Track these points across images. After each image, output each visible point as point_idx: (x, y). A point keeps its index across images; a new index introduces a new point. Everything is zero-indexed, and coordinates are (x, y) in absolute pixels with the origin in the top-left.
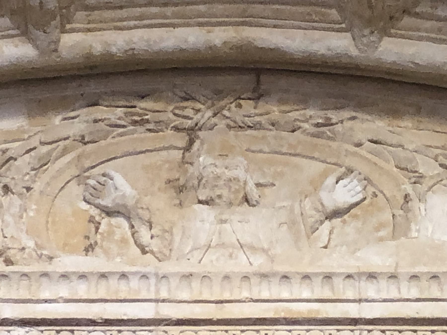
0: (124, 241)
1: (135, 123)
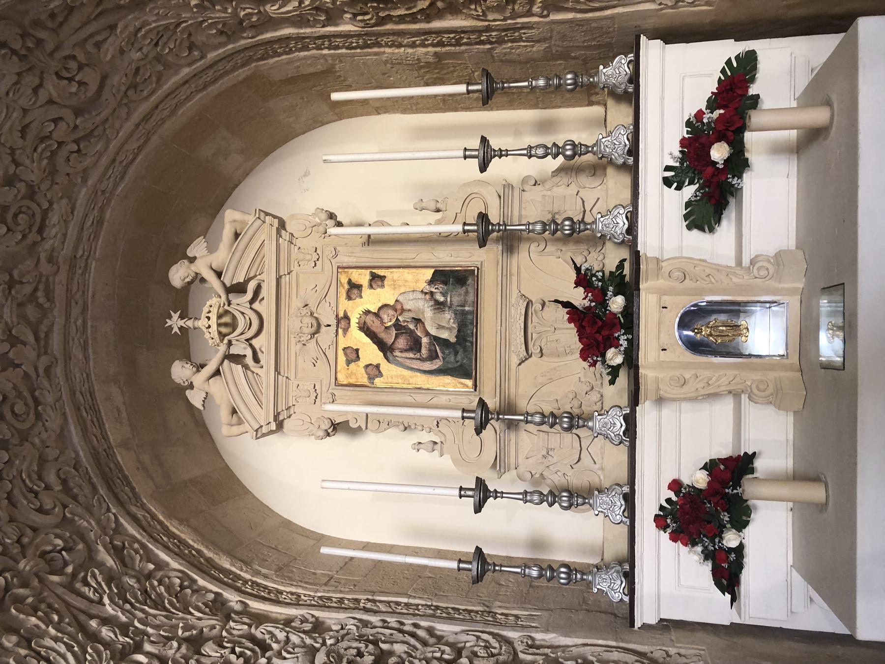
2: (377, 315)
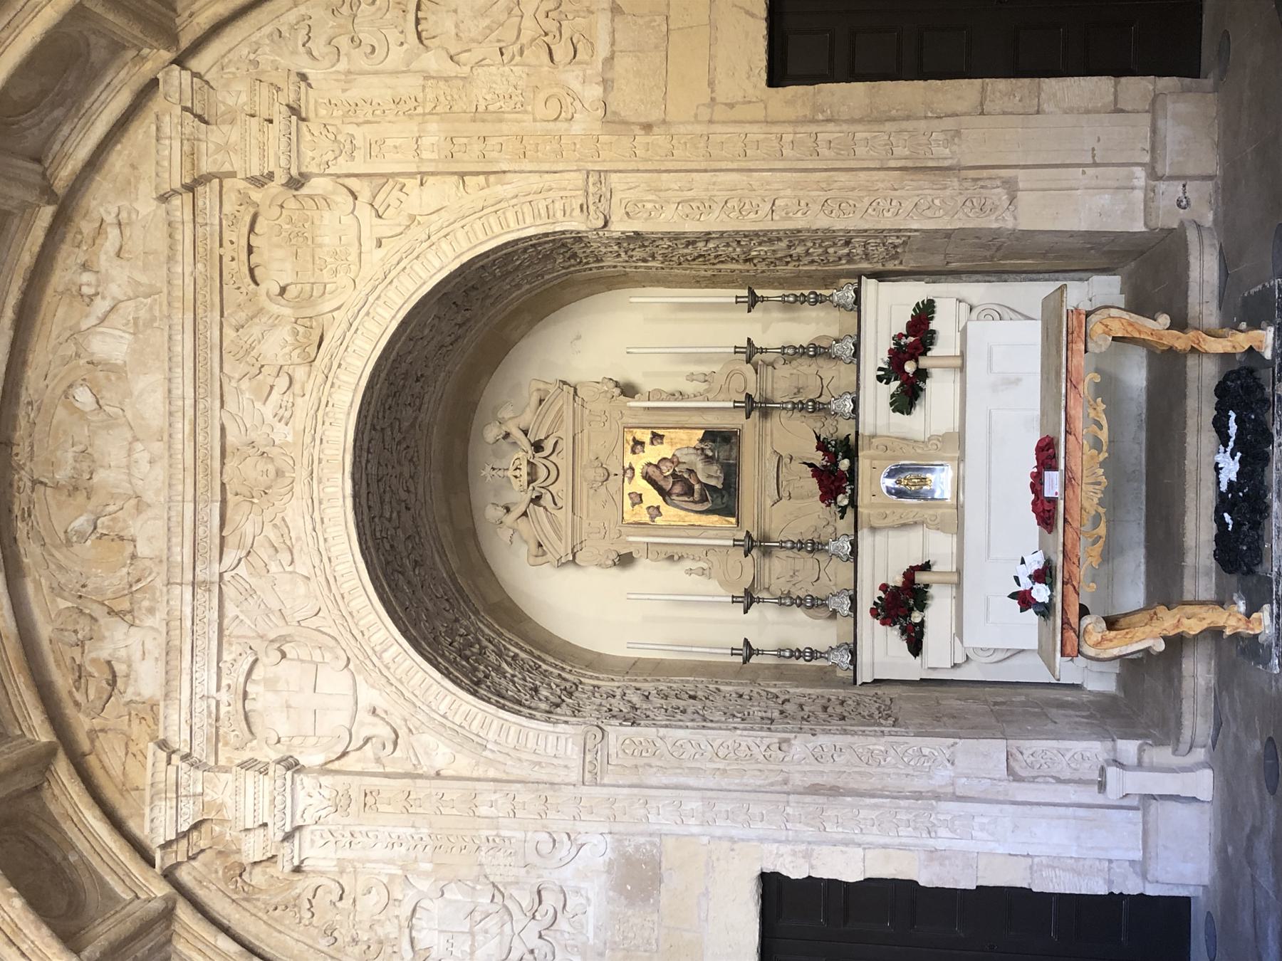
0: (112, 520)
1: (30, 515)
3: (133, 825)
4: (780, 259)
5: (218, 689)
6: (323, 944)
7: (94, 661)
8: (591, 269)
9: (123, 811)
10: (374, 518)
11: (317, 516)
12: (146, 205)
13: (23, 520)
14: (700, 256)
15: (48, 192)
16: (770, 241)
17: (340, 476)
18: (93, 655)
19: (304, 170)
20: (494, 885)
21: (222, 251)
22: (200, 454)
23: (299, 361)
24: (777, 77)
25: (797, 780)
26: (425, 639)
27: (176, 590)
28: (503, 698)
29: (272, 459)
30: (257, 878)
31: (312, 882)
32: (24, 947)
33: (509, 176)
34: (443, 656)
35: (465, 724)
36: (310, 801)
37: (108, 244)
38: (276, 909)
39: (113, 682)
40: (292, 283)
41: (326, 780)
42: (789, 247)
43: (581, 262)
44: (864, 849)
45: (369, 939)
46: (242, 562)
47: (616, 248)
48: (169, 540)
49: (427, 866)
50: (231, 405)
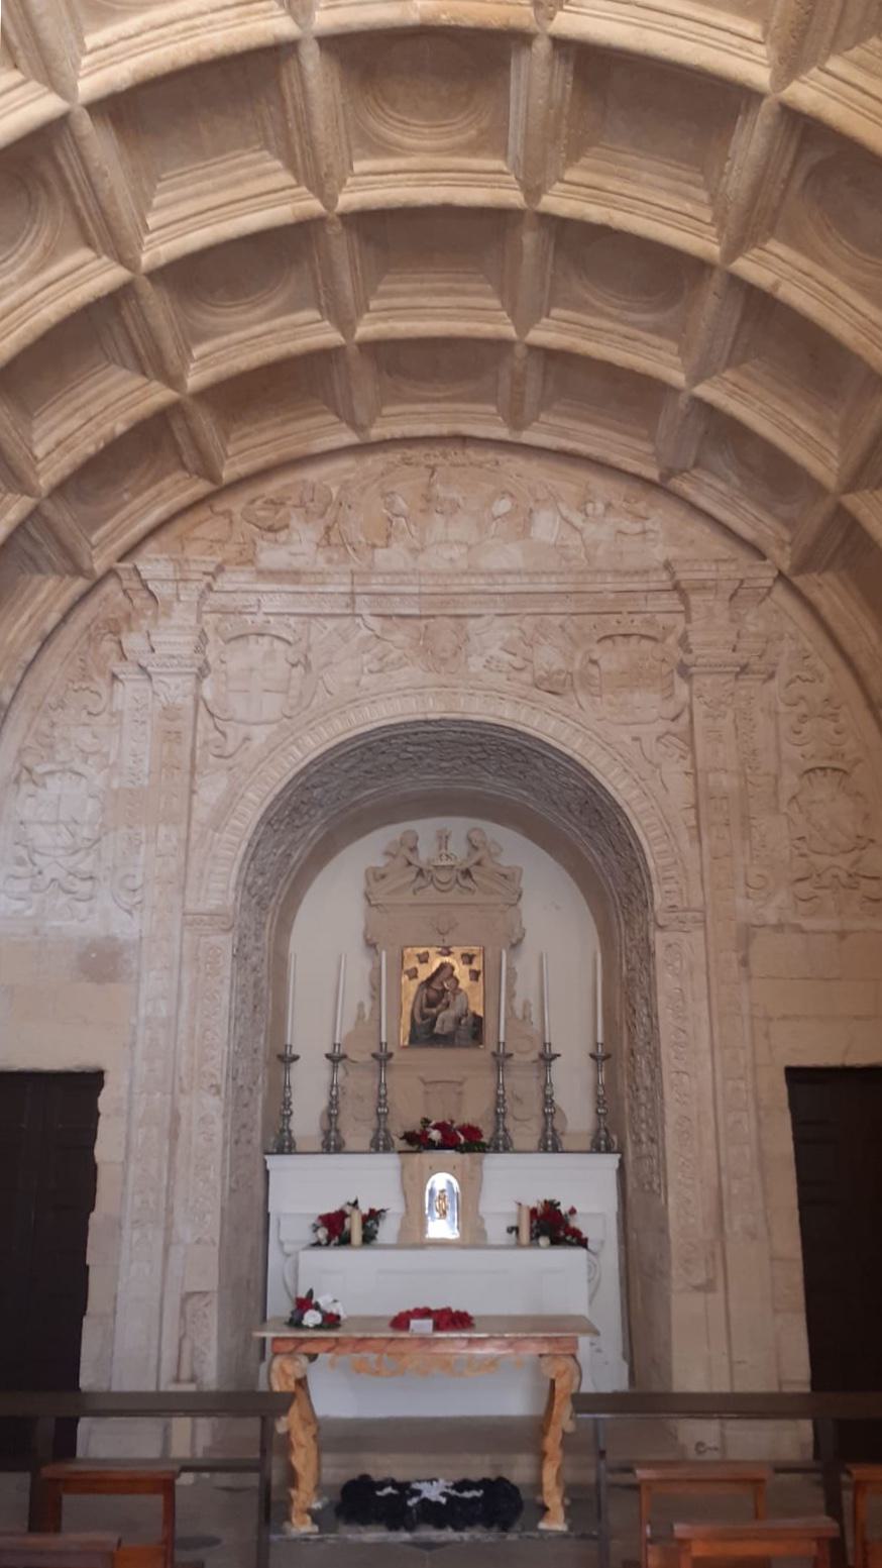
2: (452, 976)
3: (152, 544)
4: (634, 1078)
5: (266, 614)
6: (51, 699)
7: (288, 515)
8: (618, 917)
9: (165, 537)
10: (408, 737)
11: (408, 692)
12: (659, 553)
13: (403, 459)
14: (634, 1011)
15: (669, 473)
16: (652, 1071)
17: (443, 709)
18: (293, 515)
19: (695, 677)
20: (98, 840)
21: (625, 614)
22: (461, 598)
23: (537, 675)
24: (796, 1076)
25: (184, 1102)
26: (308, 779)
27: (347, 579)
28: (258, 844)
29: (455, 654)
30: (108, 645)
31: (104, 691)
32: (54, 455)
33: (697, 845)
34: (291, 795)
35: (236, 814)
36: (173, 687)
37: (627, 523)
38: (81, 660)
39: (271, 529)
40: (600, 670)
41: (189, 701)
42: (646, 1089)
43: (624, 907)
44: (123, 1163)
45: (54, 737)
46: (370, 633)
47: (638, 937)
48: (389, 574)
49: (115, 784)
50: (499, 622)
